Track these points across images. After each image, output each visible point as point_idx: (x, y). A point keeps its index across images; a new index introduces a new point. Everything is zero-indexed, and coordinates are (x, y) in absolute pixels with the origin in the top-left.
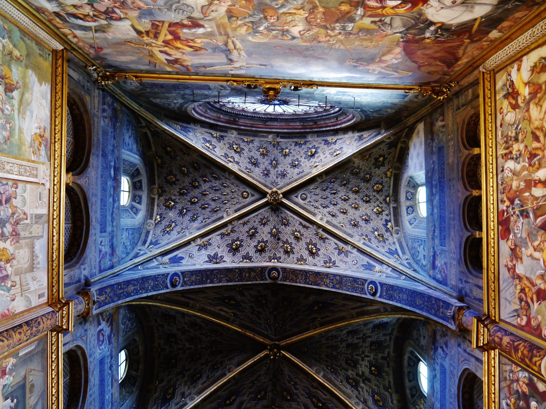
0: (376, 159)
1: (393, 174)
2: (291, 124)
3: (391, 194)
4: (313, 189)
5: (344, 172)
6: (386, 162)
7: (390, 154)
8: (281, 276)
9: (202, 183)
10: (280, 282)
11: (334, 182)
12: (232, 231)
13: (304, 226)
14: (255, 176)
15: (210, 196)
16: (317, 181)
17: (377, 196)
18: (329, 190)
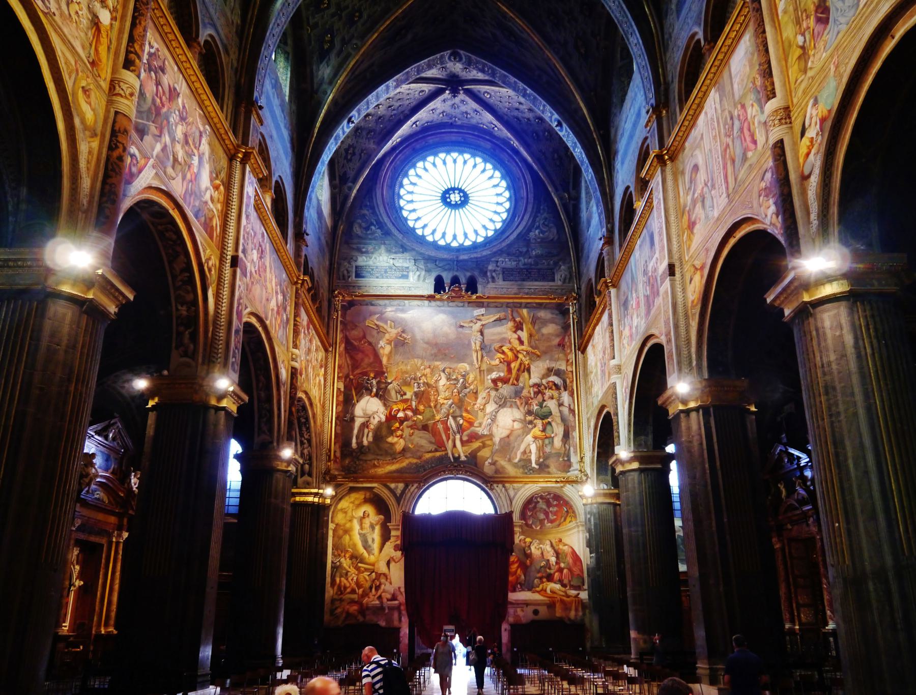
0: (354, 154)
2: (437, 140)
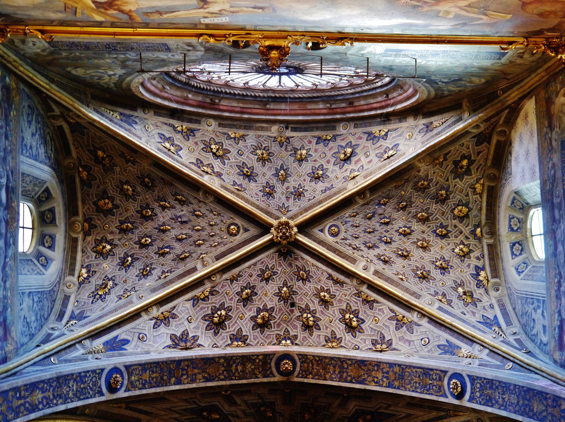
0: (456, 163)
1: (486, 188)
2: (309, 107)
3: (483, 222)
4: (350, 216)
5: (402, 185)
6: (473, 168)
7: (479, 153)
8: (298, 369)
9: (158, 210)
10: (296, 380)
11: (385, 204)
12: (212, 293)
13: (336, 282)
14: (250, 198)
15: (173, 233)
16: (357, 203)
17: (461, 226)
18: (377, 218)
